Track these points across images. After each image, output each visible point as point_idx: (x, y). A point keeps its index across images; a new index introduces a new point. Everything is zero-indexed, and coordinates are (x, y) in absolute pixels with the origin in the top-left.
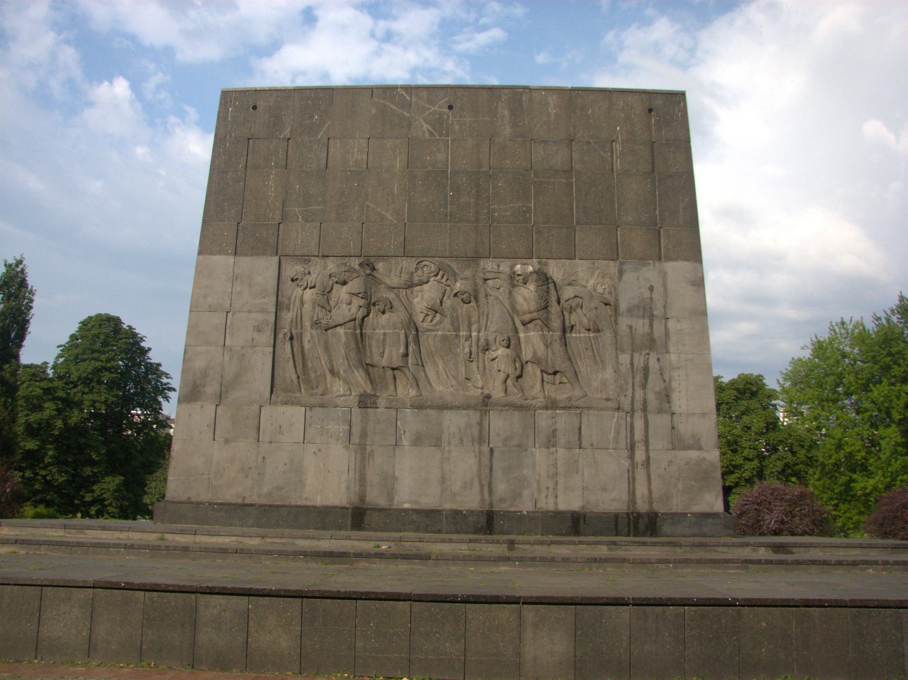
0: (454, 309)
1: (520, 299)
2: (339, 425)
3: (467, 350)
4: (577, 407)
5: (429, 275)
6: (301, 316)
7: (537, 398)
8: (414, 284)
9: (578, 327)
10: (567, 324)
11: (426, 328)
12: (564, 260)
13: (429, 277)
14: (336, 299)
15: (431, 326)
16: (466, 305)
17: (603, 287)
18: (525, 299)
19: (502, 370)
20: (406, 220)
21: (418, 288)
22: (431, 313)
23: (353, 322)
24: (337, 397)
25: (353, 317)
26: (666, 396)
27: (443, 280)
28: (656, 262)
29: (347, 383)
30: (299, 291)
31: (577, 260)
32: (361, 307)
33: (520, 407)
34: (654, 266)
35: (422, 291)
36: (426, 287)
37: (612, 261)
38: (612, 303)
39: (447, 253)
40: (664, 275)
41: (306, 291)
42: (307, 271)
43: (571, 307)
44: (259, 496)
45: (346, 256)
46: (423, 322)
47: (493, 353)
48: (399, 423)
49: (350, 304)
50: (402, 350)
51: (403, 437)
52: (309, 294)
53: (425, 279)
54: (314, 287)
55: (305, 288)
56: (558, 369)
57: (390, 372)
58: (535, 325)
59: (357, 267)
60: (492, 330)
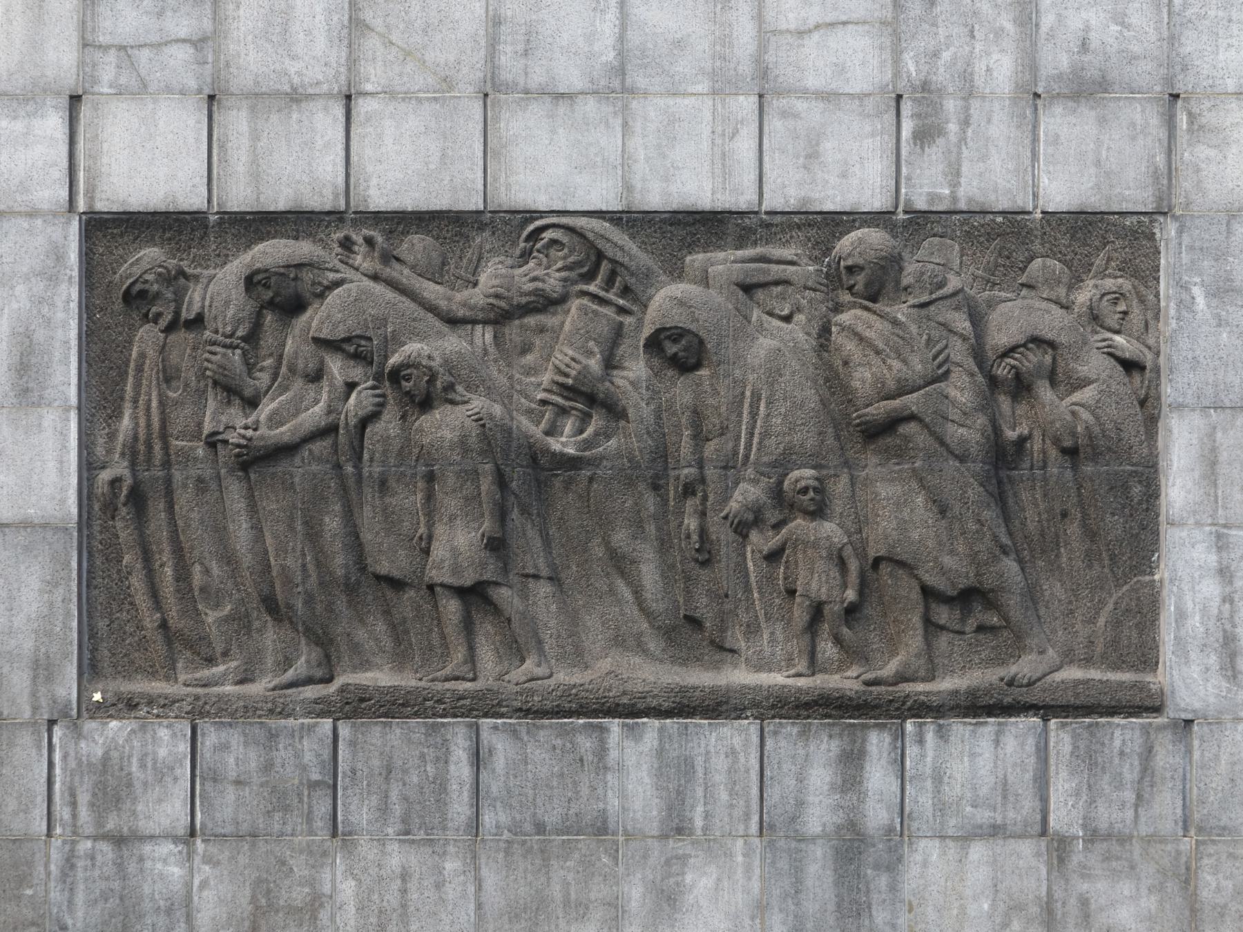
3: (692, 523)
38: (1149, 365)
41: (172, 337)
57: (452, 607)
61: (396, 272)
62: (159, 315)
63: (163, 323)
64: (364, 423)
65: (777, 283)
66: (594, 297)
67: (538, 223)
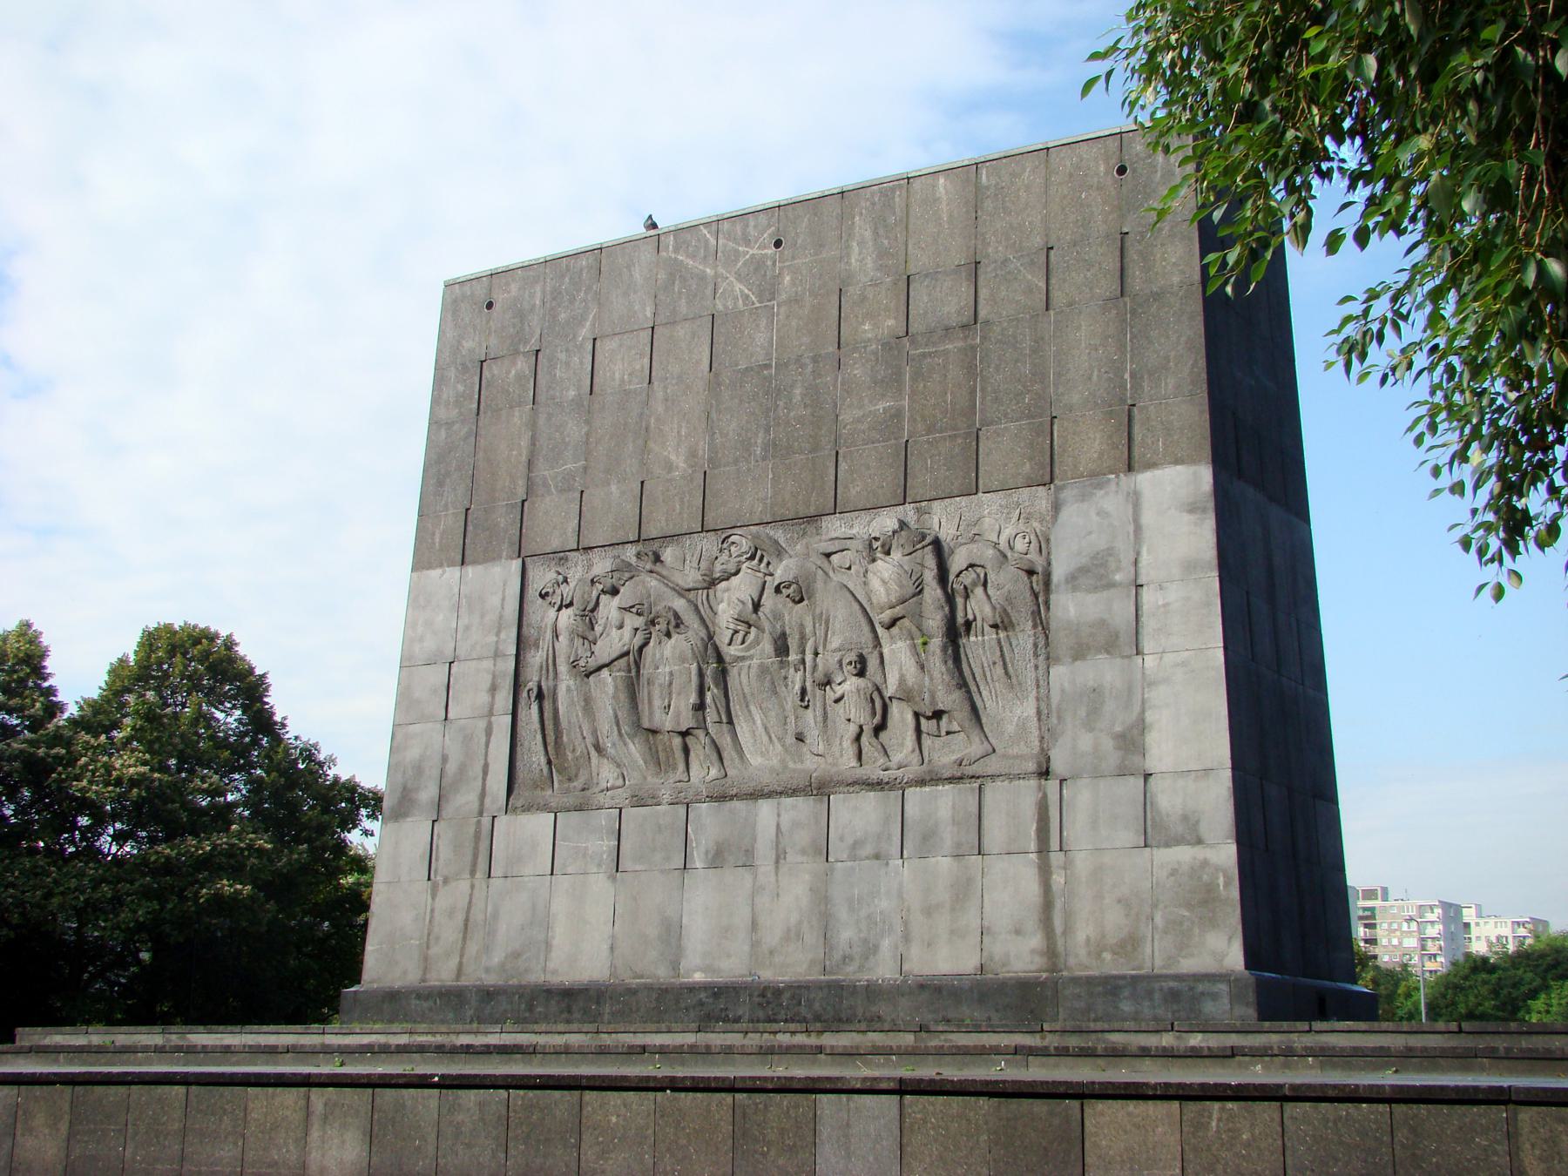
0: (777, 616)
1: (875, 583)
4: (973, 777)
5: (738, 559)
6: (554, 652)
7: (905, 766)
10: (960, 620)
12: (958, 499)
14: (604, 620)
15: (742, 650)
18: (884, 582)
21: (724, 584)
22: (742, 627)
23: (626, 658)
24: (602, 791)
25: (626, 648)
26: (1132, 740)
27: (763, 565)
28: (1122, 475)
29: (618, 766)
31: (980, 494)
32: (637, 629)
33: (879, 784)
34: (1117, 484)
35: (728, 590)
37: (1041, 488)
38: (1040, 569)
39: (768, 516)
40: (1135, 499)
42: (560, 578)
43: (965, 587)
44: (487, 970)
45: (618, 544)
46: (730, 644)
49: (621, 627)
50: (693, 698)
53: (732, 568)
54: (570, 604)
56: (941, 707)
58: (901, 629)
59: (633, 560)
61: (658, 567)
63: (556, 607)
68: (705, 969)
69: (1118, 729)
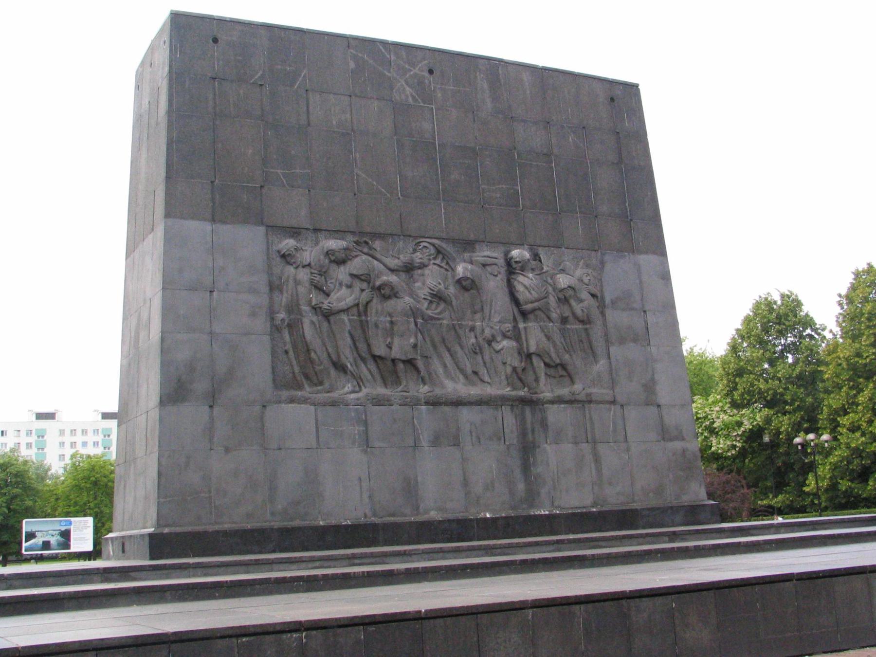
1: (520, 288)
2: (354, 426)
8: (416, 267)
9: (571, 318)
11: (431, 316)
13: (430, 260)
16: (466, 294)
17: (589, 278)
19: (508, 363)
20: (400, 194)
21: (420, 271)
25: (357, 301)
26: (650, 387)
28: (631, 254)
30: (291, 270)
32: (363, 290)
34: (629, 258)
35: (423, 275)
36: (427, 271)
38: (599, 295)
47: (498, 344)
48: (415, 422)
51: (421, 437)
52: (303, 275)
55: (297, 268)
60: (496, 320)
62: (294, 262)
64: (367, 303)
65: (493, 264)
66: (439, 266)
67: (418, 241)
68: (441, 509)
69: (643, 381)
